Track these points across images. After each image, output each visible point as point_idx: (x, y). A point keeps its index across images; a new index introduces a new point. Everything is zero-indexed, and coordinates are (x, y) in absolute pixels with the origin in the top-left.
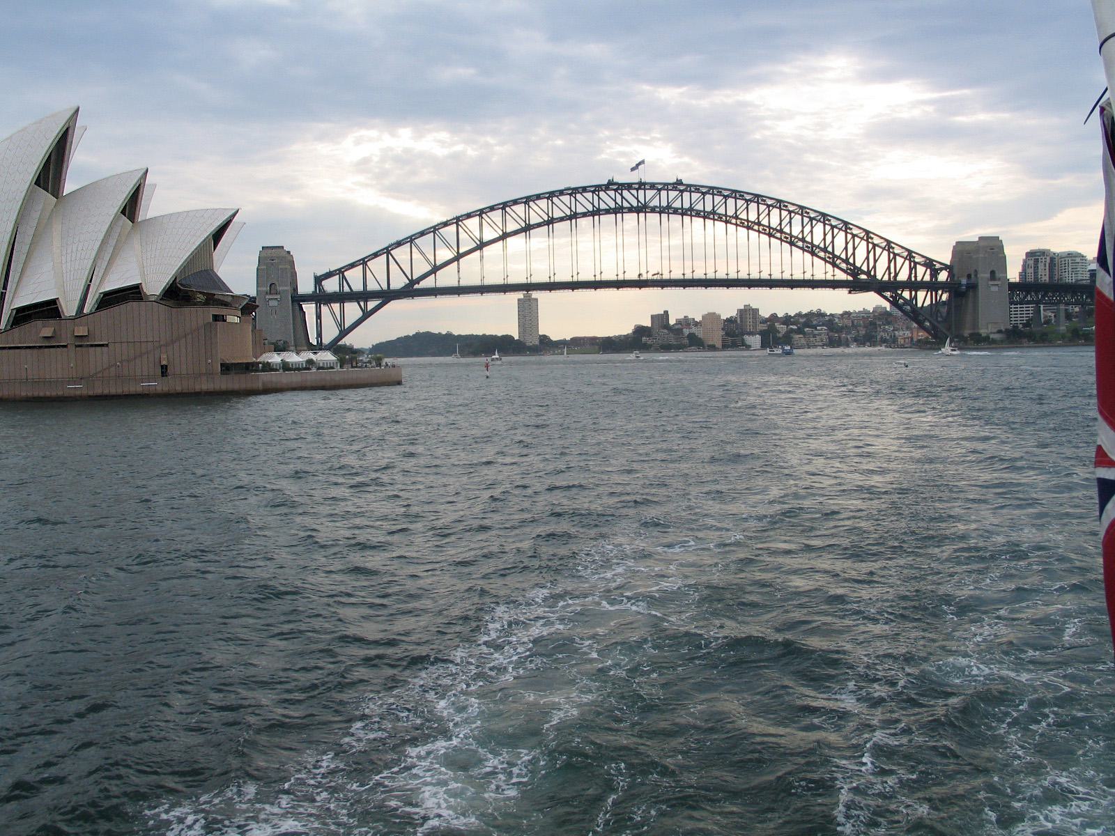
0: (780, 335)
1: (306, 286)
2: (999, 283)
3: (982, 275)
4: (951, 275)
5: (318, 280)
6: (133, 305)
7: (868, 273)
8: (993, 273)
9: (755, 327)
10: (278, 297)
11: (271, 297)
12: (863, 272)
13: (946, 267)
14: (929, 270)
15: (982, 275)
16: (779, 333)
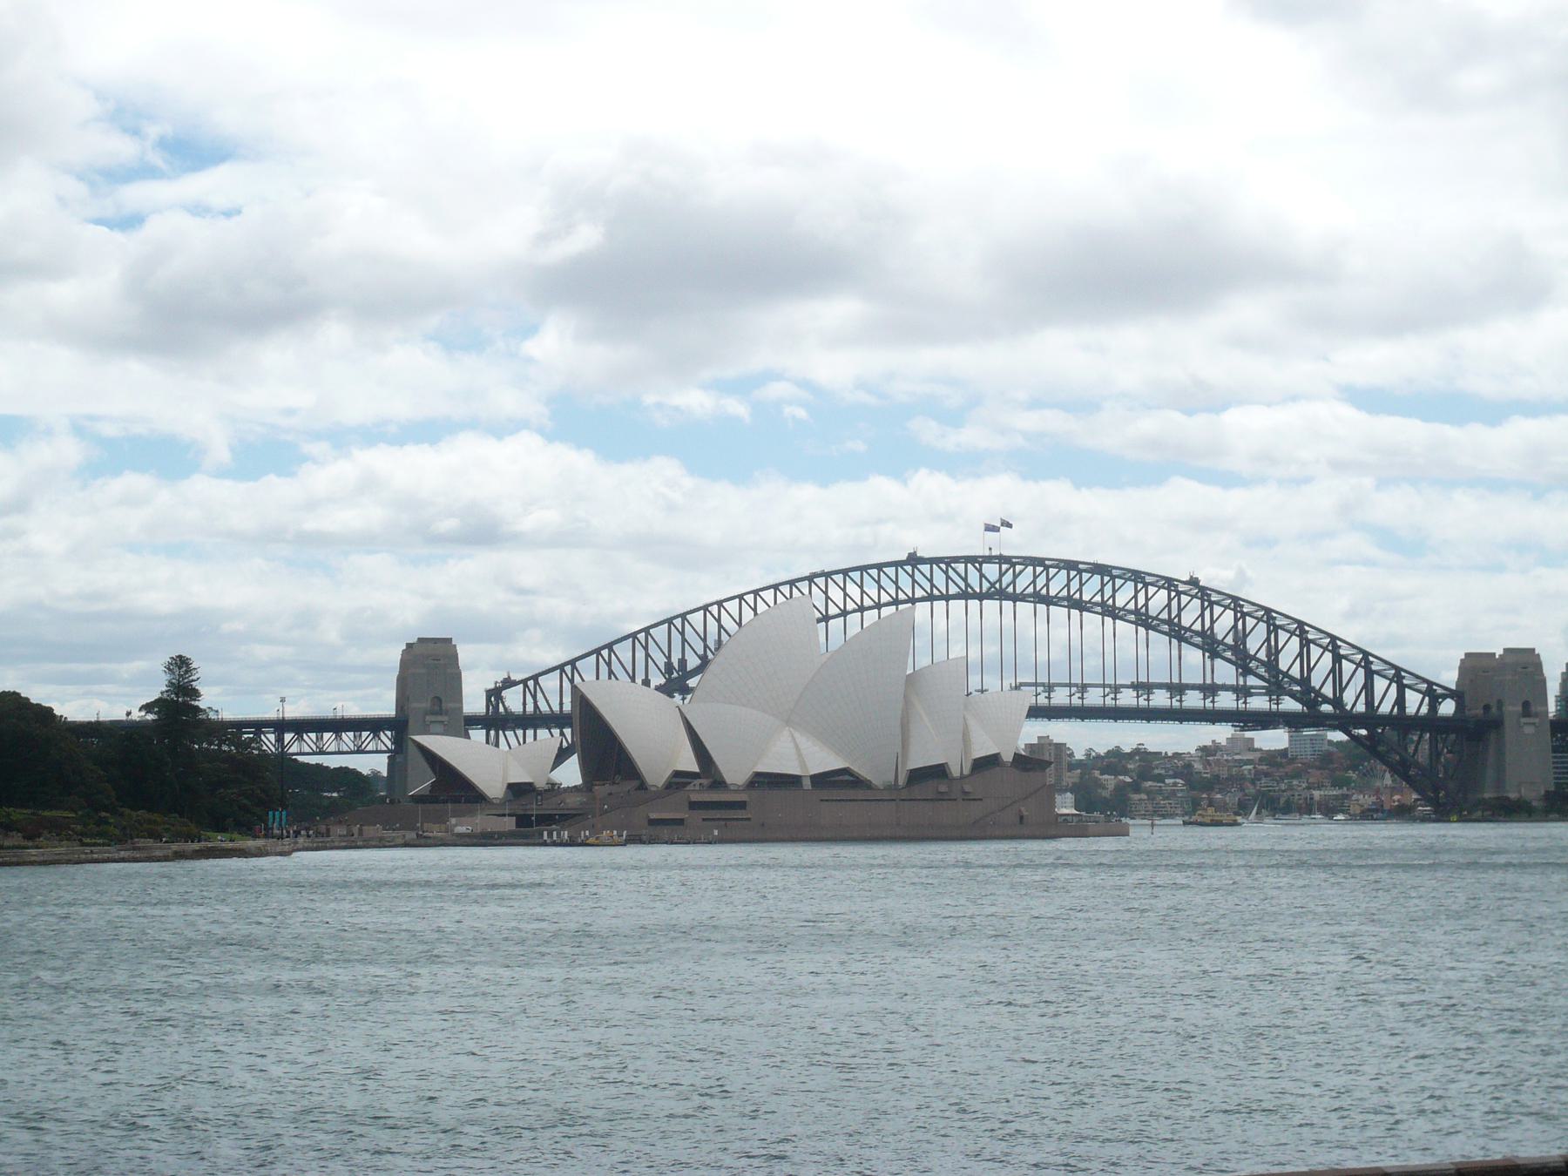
0: (1105, 794)
1: (474, 703)
2: (1536, 720)
3: (1511, 708)
4: (1460, 707)
5: (494, 694)
6: (998, 768)
7: (1337, 702)
8: (1526, 705)
9: (1059, 778)
10: (445, 718)
11: (433, 718)
12: (1326, 700)
13: (1450, 694)
14: (1427, 699)
15: (1511, 708)
16: (1104, 788)
